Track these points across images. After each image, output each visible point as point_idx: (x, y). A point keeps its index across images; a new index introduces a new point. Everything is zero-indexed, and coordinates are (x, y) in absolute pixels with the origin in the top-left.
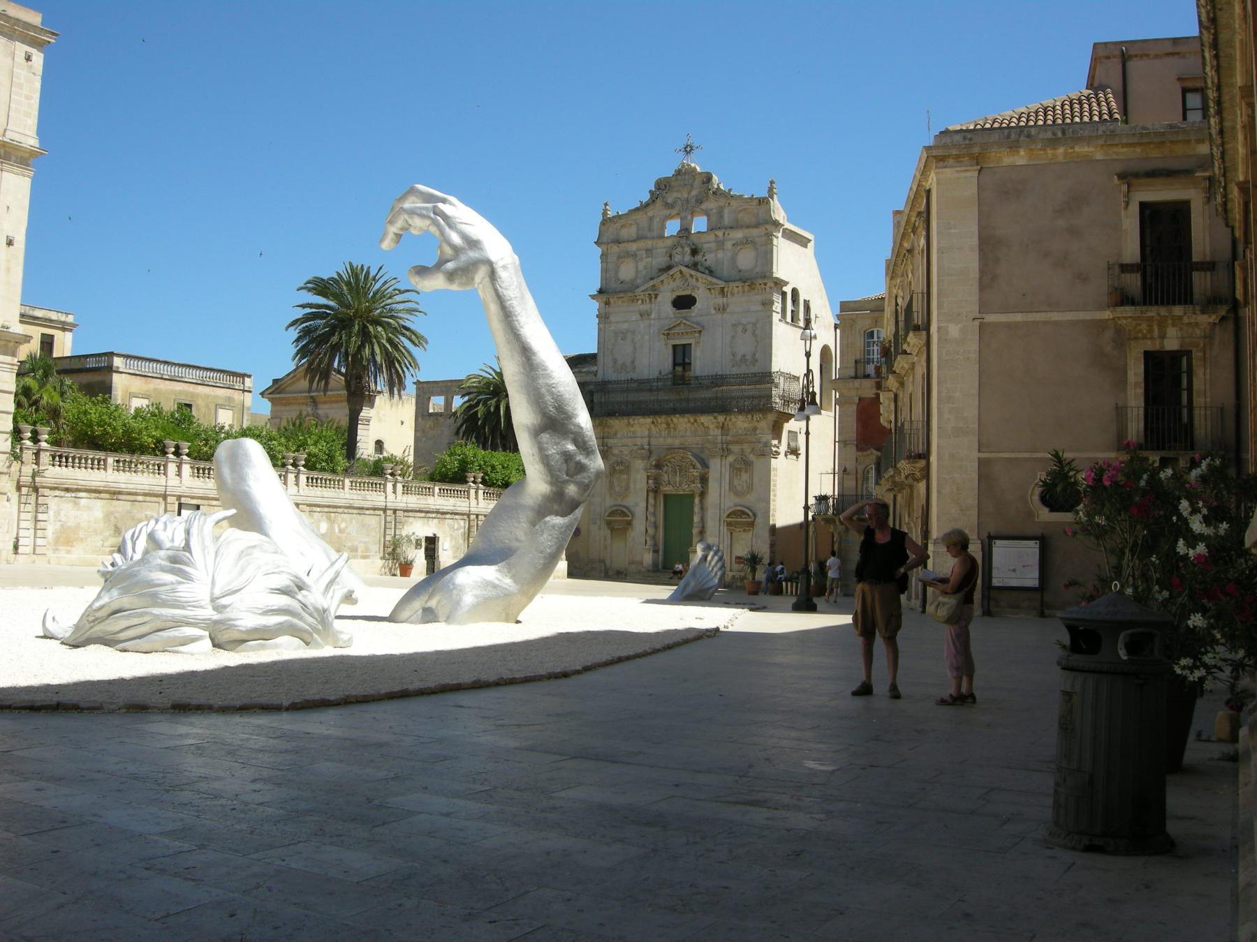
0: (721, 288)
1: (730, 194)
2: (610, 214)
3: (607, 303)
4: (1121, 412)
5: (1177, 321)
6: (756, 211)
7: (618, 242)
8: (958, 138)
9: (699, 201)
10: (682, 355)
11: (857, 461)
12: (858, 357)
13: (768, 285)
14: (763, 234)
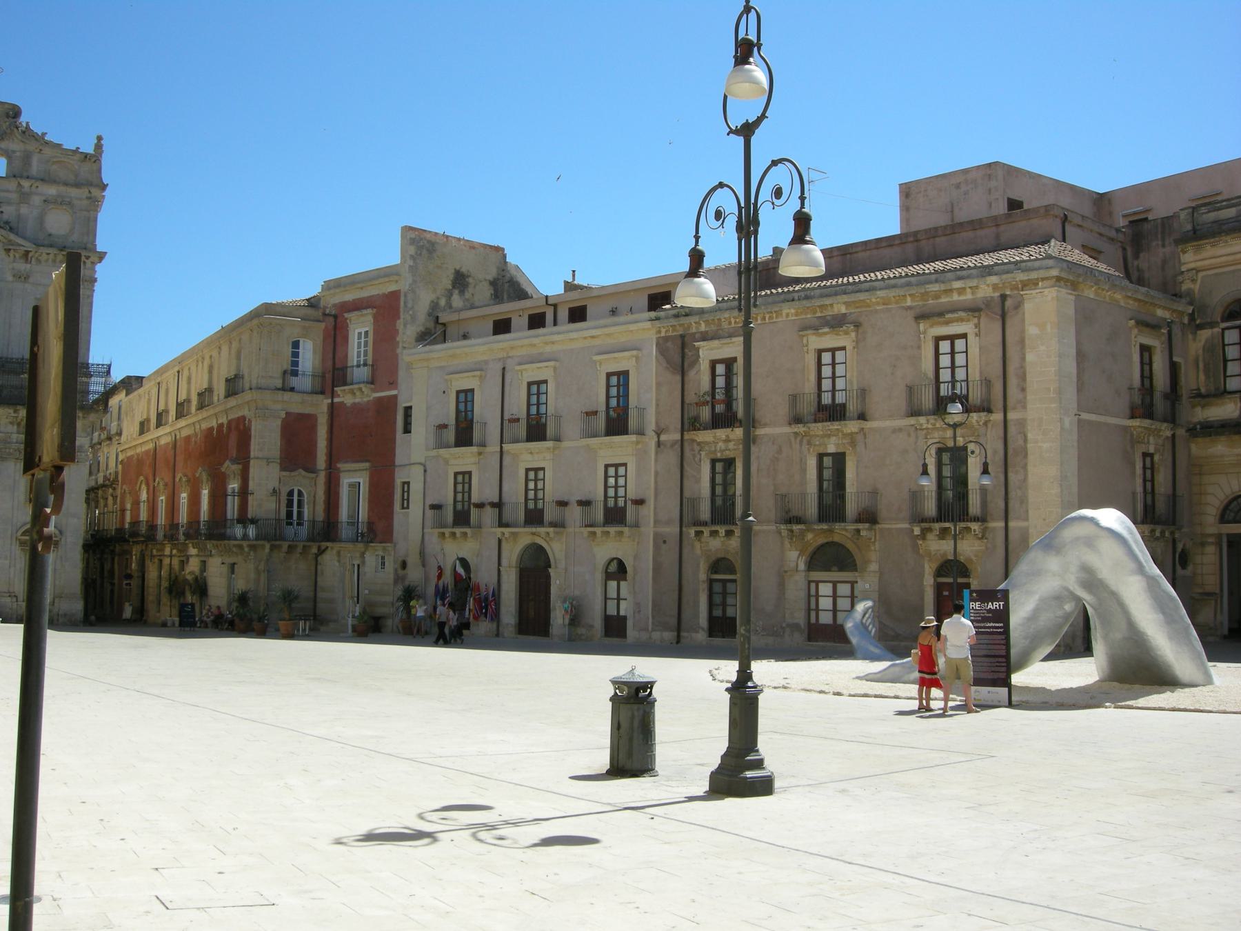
0: (26, 251)
1: (43, 139)
4: (1134, 494)
6: (77, 167)
8: (1065, 265)
11: (280, 483)
12: (285, 367)
13: (91, 260)
14: (84, 197)
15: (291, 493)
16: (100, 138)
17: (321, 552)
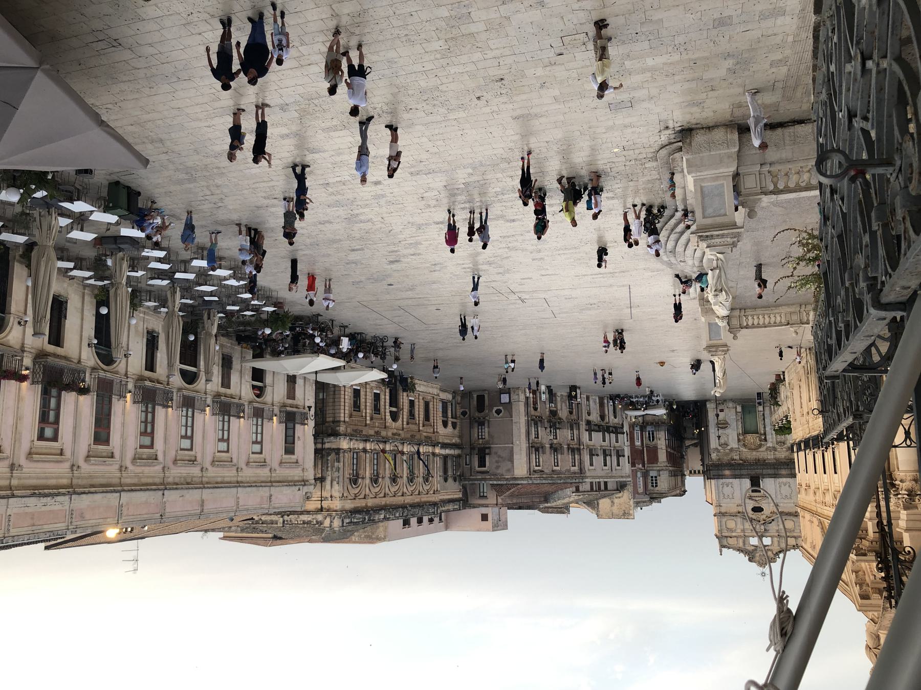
4: (489, 427)
5: (479, 444)
15: (653, 440)
16: (721, 554)
17: (643, 423)
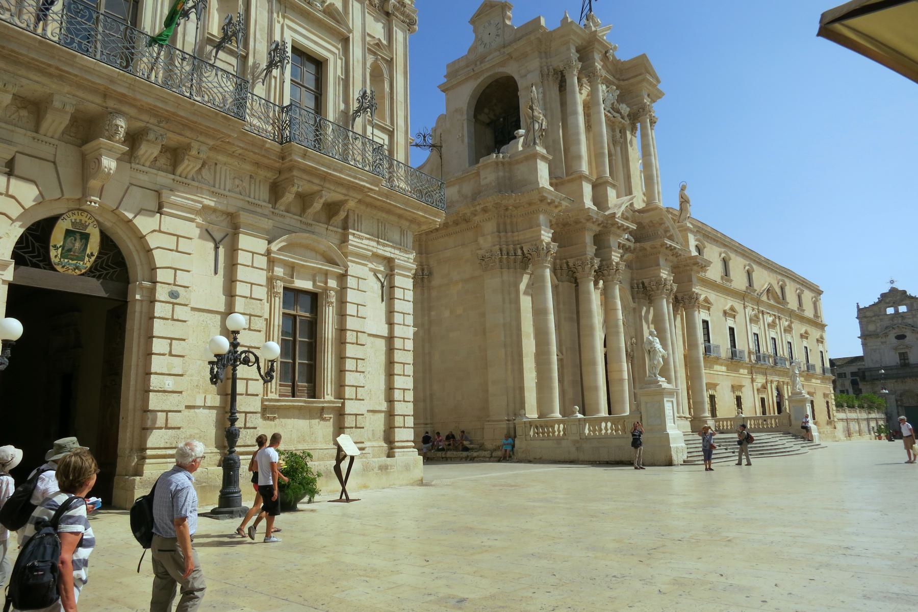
2: (861, 307)
3: (865, 339)
7: (865, 317)
9: (902, 301)
10: (903, 356)
